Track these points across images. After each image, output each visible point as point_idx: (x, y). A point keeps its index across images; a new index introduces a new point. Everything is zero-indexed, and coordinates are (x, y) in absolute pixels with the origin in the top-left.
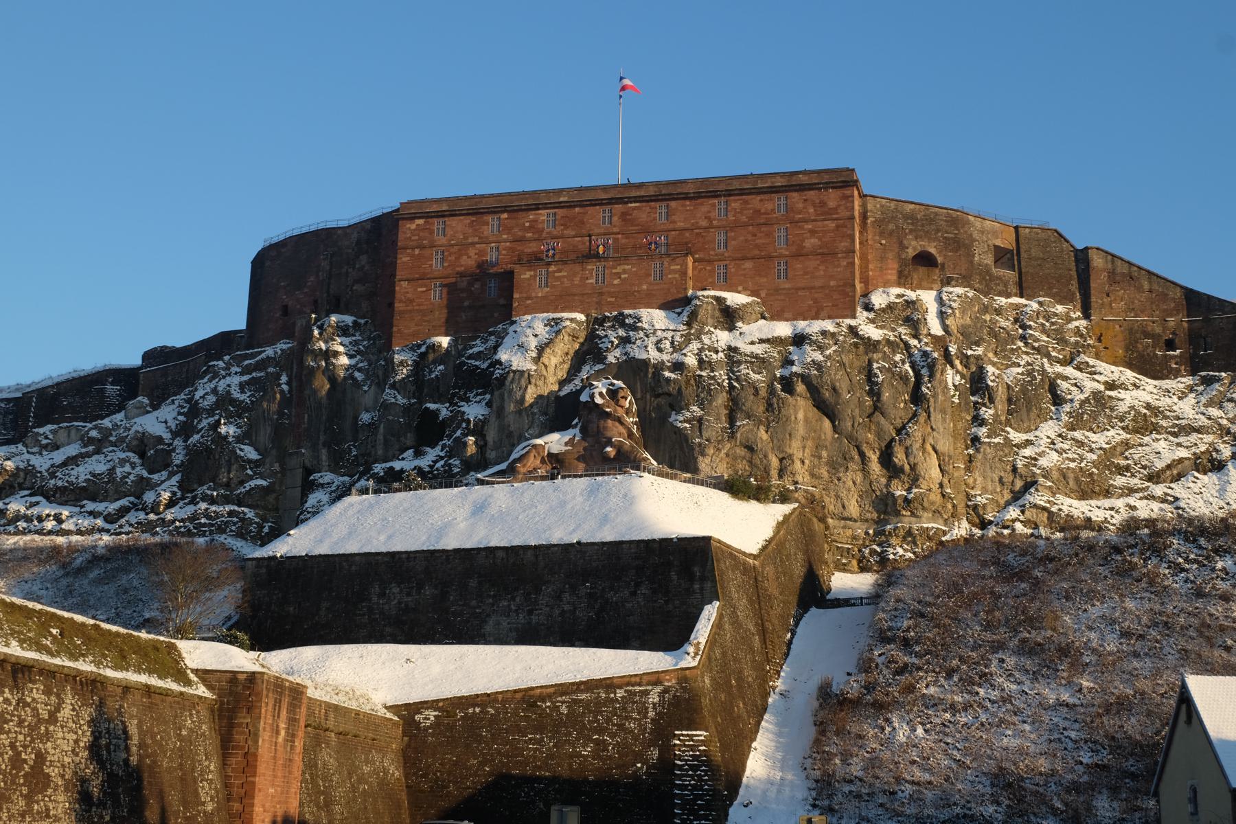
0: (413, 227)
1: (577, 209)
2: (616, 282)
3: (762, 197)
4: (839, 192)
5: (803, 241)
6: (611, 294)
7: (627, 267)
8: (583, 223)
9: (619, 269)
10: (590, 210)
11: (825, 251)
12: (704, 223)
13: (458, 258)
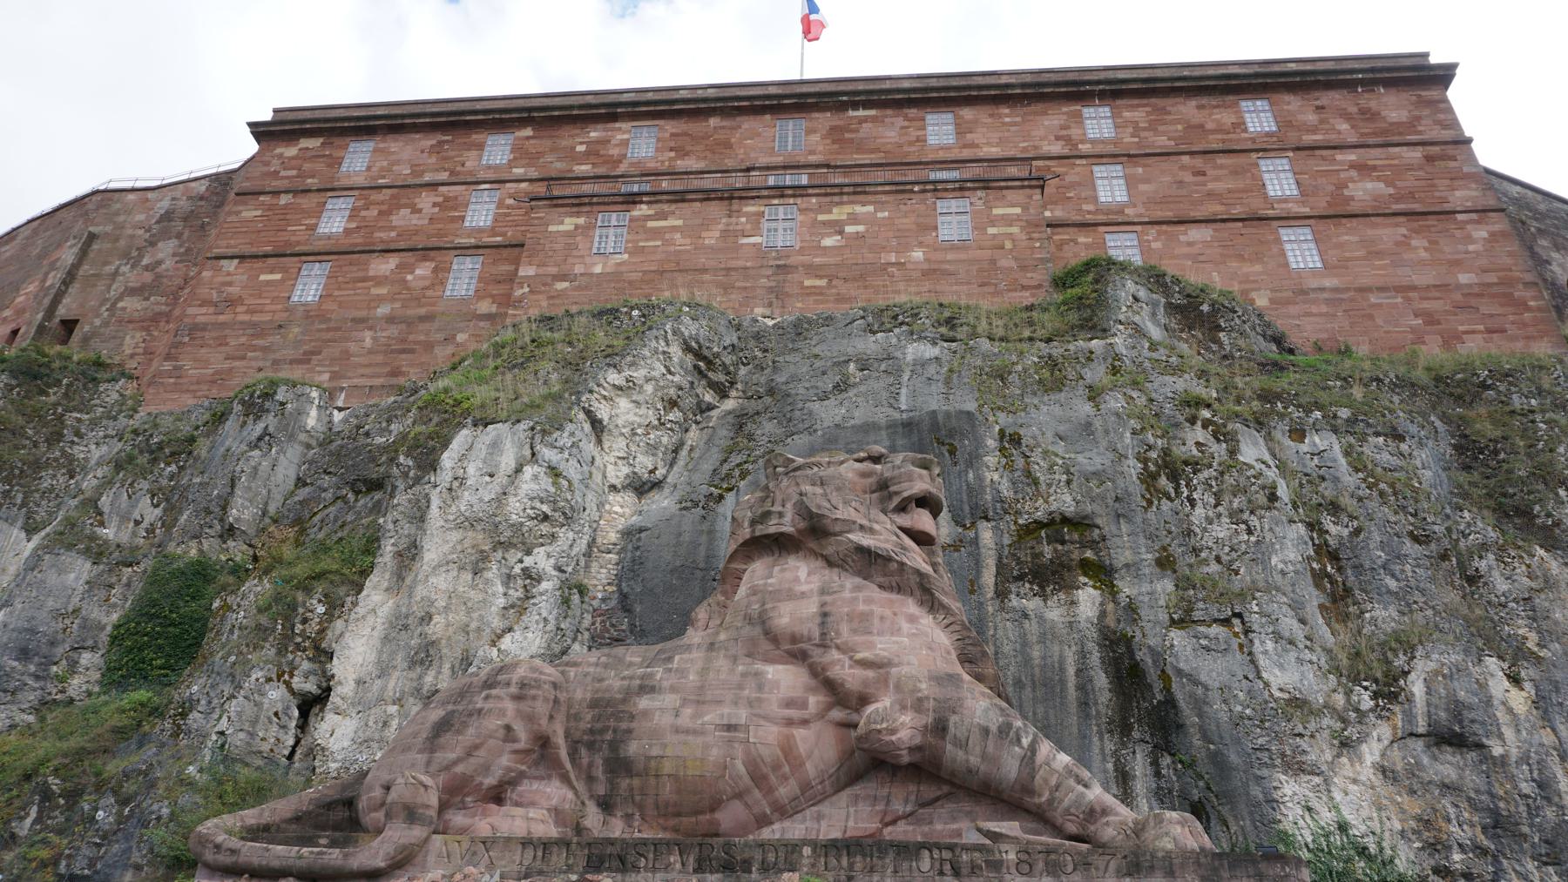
0: (291, 151)
1: (714, 121)
3: (1204, 101)
5: (1342, 186)
6: (813, 271)
7: (859, 209)
8: (728, 145)
9: (838, 213)
10: (748, 124)
11: (1417, 207)
12: (1056, 148)
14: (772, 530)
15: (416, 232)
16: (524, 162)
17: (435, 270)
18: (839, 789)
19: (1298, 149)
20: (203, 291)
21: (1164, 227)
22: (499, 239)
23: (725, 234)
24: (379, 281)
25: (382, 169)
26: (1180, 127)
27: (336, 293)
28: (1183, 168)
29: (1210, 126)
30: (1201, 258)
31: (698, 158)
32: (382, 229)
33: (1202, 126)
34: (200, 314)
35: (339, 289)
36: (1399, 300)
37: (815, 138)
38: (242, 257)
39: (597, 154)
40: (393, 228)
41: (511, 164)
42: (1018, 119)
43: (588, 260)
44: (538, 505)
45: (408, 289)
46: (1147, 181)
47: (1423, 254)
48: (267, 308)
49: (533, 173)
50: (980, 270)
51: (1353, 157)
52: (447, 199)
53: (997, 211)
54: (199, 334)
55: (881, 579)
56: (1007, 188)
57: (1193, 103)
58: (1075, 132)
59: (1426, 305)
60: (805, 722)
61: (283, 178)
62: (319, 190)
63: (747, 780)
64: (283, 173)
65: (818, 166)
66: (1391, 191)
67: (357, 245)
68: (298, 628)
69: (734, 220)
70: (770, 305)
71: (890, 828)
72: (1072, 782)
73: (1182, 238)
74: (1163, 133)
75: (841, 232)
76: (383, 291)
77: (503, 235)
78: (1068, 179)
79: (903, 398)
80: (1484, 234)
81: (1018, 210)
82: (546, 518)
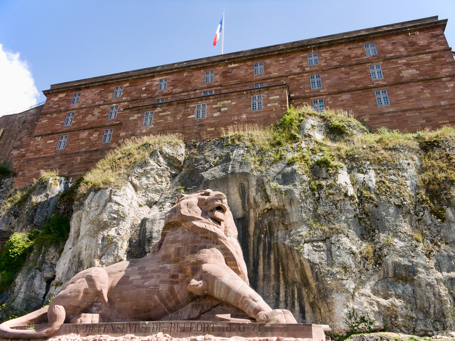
0: (56, 99)
2: (216, 115)
4: (428, 34)
6: (211, 125)
7: (226, 102)
8: (189, 82)
9: (219, 105)
10: (196, 73)
11: (427, 77)
12: (298, 70)
13: (84, 117)
14: (173, 220)
15: (94, 122)
16: (126, 95)
17: (99, 135)
18: (188, 302)
19: (384, 60)
20: (31, 148)
21: (334, 95)
22: (118, 122)
23: (184, 115)
24: (82, 140)
25: (83, 102)
26: (341, 57)
27: (70, 145)
28: (342, 72)
29: (353, 55)
30: (346, 105)
31: (180, 88)
32: (83, 122)
33: (349, 56)
34: (30, 155)
35: (71, 144)
36: (418, 114)
37: (217, 76)
38: (41, 136)
39: (148, 90)
40: (86, 122)
41: (123, 96)
42: (285, 61)
43: (141, 128)
44: (112, 215)
45: (91, 142)
46: (329, 79)
47: (428, 95)
48: (50, 152)
49: (129, 99)
50: (264, 119)
51: (405, 61)
52: (103, 110)
53: (271, 98)
54: (30, 162)
55: (202, 235)
56: (275, 89)
57: (347, 48)
58: (305, 64)
59: (427, 115)
60: (177, 282)
61: (55, 108)
62: (64, 111)
63: (159, 301)
64: (54, 107)
65: (218, 86)
66: (418, 72)
67: (76, 128)
68: (46, 258)
69: (186, 110)
70: (196, 138)
71: (203, 315)
72: (251, 300)
73: (340, 99)
74: (335, 61)
75: (220, 111)
76: (83, 143)
77: (120, 121)
78: (301, 81)
79: (230, 169)
80: (452, 85)
81: (278, 97)
82: (115, 218)
